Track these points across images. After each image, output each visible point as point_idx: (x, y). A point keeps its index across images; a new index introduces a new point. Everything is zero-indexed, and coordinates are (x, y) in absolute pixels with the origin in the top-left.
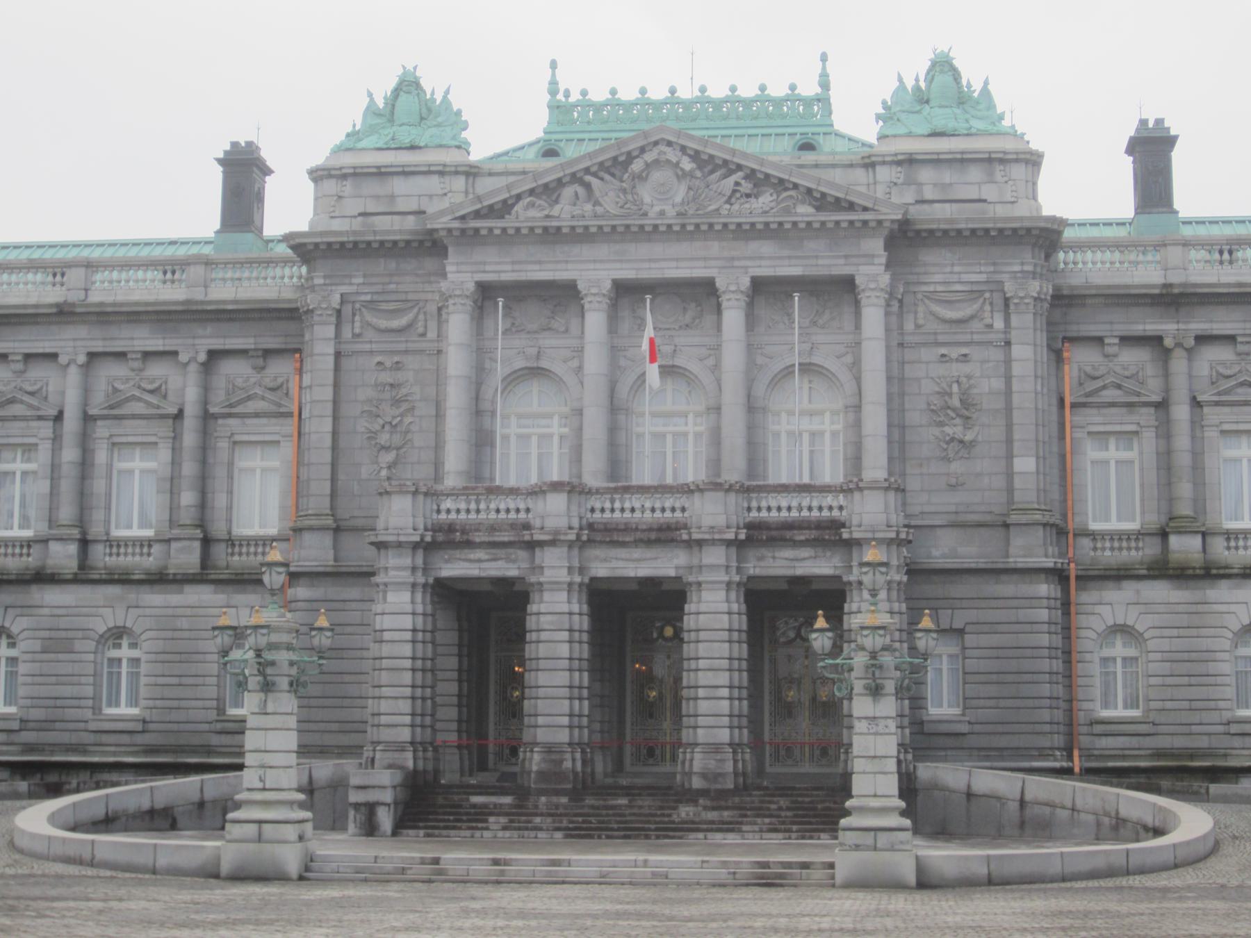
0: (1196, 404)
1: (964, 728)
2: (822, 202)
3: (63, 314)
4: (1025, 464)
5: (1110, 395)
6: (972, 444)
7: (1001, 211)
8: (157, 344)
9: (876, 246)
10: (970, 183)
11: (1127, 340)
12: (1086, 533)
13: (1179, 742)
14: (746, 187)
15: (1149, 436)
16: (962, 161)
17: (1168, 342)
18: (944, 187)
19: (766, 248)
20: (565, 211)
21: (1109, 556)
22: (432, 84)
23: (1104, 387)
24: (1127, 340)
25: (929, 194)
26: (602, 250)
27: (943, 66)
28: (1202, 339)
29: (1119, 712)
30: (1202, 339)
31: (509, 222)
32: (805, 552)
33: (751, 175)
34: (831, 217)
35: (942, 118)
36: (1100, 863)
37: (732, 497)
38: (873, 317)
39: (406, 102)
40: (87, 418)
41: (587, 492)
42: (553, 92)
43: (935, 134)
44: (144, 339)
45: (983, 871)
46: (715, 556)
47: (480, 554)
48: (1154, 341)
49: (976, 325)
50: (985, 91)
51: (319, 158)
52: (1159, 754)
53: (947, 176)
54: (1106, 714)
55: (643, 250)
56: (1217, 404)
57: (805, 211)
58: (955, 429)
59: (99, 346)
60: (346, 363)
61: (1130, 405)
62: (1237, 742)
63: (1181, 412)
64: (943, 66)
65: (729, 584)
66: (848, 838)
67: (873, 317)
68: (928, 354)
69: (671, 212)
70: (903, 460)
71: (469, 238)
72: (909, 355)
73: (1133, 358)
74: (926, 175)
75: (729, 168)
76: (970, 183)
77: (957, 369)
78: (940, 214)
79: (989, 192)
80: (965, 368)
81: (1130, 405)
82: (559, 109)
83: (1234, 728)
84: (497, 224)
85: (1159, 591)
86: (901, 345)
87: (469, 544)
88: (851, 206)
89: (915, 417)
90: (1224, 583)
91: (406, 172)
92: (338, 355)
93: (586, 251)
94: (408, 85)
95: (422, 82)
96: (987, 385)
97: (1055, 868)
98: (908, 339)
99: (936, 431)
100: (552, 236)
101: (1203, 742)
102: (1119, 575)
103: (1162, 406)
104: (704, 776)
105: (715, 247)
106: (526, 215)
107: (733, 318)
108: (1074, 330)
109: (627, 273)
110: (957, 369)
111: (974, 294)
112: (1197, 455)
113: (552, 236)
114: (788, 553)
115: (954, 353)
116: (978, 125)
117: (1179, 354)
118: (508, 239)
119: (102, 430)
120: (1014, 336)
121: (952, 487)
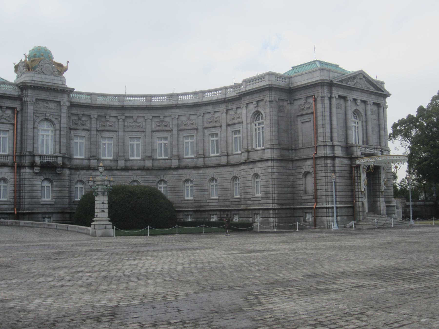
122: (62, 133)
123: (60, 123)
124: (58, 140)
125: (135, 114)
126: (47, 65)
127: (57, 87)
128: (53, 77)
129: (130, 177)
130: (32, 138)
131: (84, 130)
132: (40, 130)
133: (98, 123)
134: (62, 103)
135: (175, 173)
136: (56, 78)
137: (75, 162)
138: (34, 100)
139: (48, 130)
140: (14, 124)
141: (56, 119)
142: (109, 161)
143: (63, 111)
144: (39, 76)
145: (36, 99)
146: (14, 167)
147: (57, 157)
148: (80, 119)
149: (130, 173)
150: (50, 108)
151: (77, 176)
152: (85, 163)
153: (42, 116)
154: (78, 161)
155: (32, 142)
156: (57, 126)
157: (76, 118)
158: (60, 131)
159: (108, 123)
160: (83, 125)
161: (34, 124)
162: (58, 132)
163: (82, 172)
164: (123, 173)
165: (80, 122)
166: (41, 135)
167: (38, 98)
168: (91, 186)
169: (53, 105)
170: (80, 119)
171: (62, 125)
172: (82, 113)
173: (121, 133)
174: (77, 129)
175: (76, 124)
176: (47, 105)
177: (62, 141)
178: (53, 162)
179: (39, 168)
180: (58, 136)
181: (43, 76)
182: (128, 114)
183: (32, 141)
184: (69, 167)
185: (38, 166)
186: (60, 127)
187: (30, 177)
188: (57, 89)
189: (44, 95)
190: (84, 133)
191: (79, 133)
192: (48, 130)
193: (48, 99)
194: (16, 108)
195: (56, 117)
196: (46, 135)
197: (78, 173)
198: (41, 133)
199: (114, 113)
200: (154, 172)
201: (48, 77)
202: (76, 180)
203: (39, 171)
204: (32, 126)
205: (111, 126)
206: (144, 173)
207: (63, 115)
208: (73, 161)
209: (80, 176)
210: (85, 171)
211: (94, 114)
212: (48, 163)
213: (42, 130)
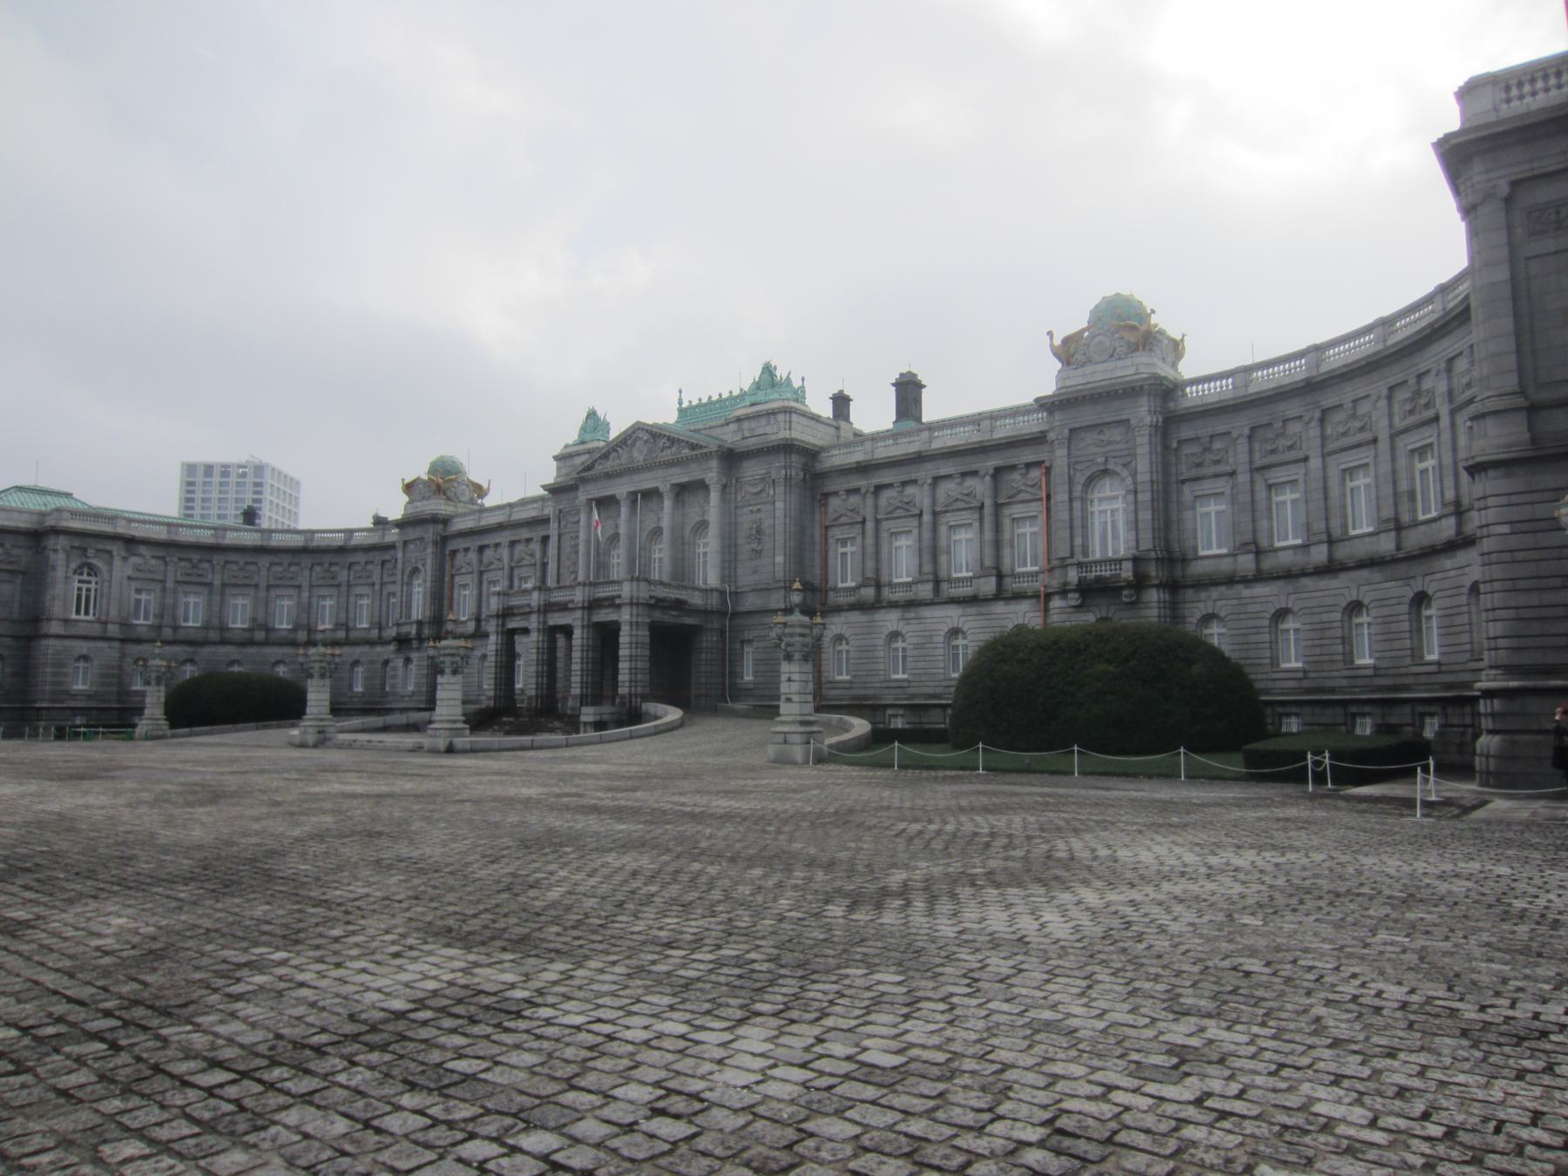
0: (877, 522)
1: (752, 686)
2: (693, 447)
3: (500, 527)
4: (779, 559)
5: (844, 520)
6: (761, 551)
7: (773, 437)
8: (528, 535)
9: (714, 463)
10: (762, 427)
11: (850, 492)
12: (835, 589)
13: (863, 692)
14: (668, 444)
15: (859, 539)
16: (756, 416)
17: (863, 491)
18: (751, 430)
19: (676, 470)
20: (609, 465)
21: (842, 600)
22: (600, 413)
23: (840, 516)
24: (850, 492)
25: (747, 434)
26: (624, 480)
27: (768, 370)
28: (879, 488)
29: (845, 677)
30: (879, 488)
31: (593, 472)
32: (610, 610)
33: (669, 439)
34: (698, 452)
35: (760, 397)
36: (518, 745)
37: (587, 588)
38: (714, 496)
39: (591, 422)
40: (512, 569)
41: (549, 590)
42: (680, 403)
43: (752, 405)
44: (524, 534)
45: (468, 746)
46: (578, 614)
47: (518, 618)
48: (856, 491)
49: (764, 494)
50: (788, 378)
51: (557, 451)
52: (854, 698)
53: (753, 424)
54: (839, 678)
55: (637, 477)
56: (888, 519)
57: (686, 452)
58: (754, 546)
59: (513, 538)
60: (563, 538)
61: (852, 524)
62: (886, 691)
63: (870, 525)
64: (768, 370)
65: (583, 626)
66: (429, 732)
67: (714, 496)
68: (746, 510)
69: (641, 458)
70: (736, 560)
71: (584, 481)
72: (739, 511)
73: (854, 500)
74: (746, 425)
75: (661, 436)
76: (762, 427)
77: (754, 517)
78: (752, 443)
79: (768, 430)
80: (759, 515)
81: (852, 524)
82: (681, 411)
83: (884, 685)
84: (589, 473)
85: (856, 617)
86: (736, 508)
87: (514, 615)
88: (701, 447)
89: (741, 541)
90: (883, 611)
91: (578, 454)
92: (560, 536)
93: (618, 481)
94: (592, 415)
95: (599, 413)
96: (767, 523)
97: (496, 746)
98: (739, 504)
99: (748, 547)
100: (608, 476)
101: (871, 692)
102: (838, 609)
103: (863, 522)
104: (572, 709)
105: (660, 473)
106: (599, 468)
107: (667, 503)
108: (826, 490)
109: (633, 489)
110: (754, 517)
111: (763, 480)
112: (877, 545)
113: (608, 476)
114: (604, 611)
115: (755, 509)
116: (776, 396)
117: (869, 495)
118: (596, 479)
119: (516, 572)
120: (777, 497)
121: (755, 572)
122: (1141, 497)
123: (1134, 474)
124: (1132, 518)
125: (1347, 393)
126: (1098, 339)
127: (1113, 385)
128: (1110, 365)
129: (1341, 591)
130: (1068, 525)
131: (1216, 476)
132: (1096, 501)
133: (1257, 447)
134: (1133, 422)
135: (1448, 563)
136: (1120, 363)
137: (1197, 569)
138: (1066, 432)
139: (1116, 498)
140: (1041, 499)
141: (1124, 465)
142: (1291, 552)
143: (1139, 440)
144: (1080, 371)
145: (1071, 430)
146: (1039, 597)
147: (1120, 561)
148: (1207, 449)
149: (1343, 580)
150: (1109, 443)
151: (1201, 605)
152: (1226, 566)
153: (1088, 467)
154: (1206, 562)
155: (1067, 534)
156: (1129, 481)
157: (1195, 449)
158: (1136, 492)
159: (1283, 443)
160: (1217, 462)
161: (1070, 492)
162: (1131, 498)
163: (1215, 592)
164: (1324, 583)
165: (1209, 457)
166: (1100, 512)
167: (1077, 425)
168: (302, 664)
169: (1116, 434)
170: (1207, 449)
171: (1140, 478)
172: (1210, 431)
173: (1315, 463)
174: (1196, 479)
175: (1199, 465)
176: (1101, 437)
177: (1140, 517)
178: (1112, 576)
179: (1077, 595)
180: (1132, 508)
181: (1089, 369)
182: (1328, 400)
183: (1068, 531)
184: (1157, 582)
185: (1074, 591)
186: (1135, 483)
187: (1064, 617)
188: (1116, 391)
189: (1088, 415)
190: (1221, 485)
191: (1206, 487)
192: (1116, 498)
193: (1100, 421)
194: (1043, 462)
195: (1126, 460)
196: (1113, 511)
197: (1203, 595)
198: (1096, 507)
199: (1292, 408)
200: (1402, 569)
201: (1100, 367)
202: (1198, 615)
203: (1079, 602)
204: (1066, 497)
205: (1291, 448)
206: (1376, 575)
207: (1139, 451)
208: (1194, 563)
209: (1210, 604)
210: (1222, 589)
211: (1240, 425)
212: (1098, 579)
213: (1101, 500)
